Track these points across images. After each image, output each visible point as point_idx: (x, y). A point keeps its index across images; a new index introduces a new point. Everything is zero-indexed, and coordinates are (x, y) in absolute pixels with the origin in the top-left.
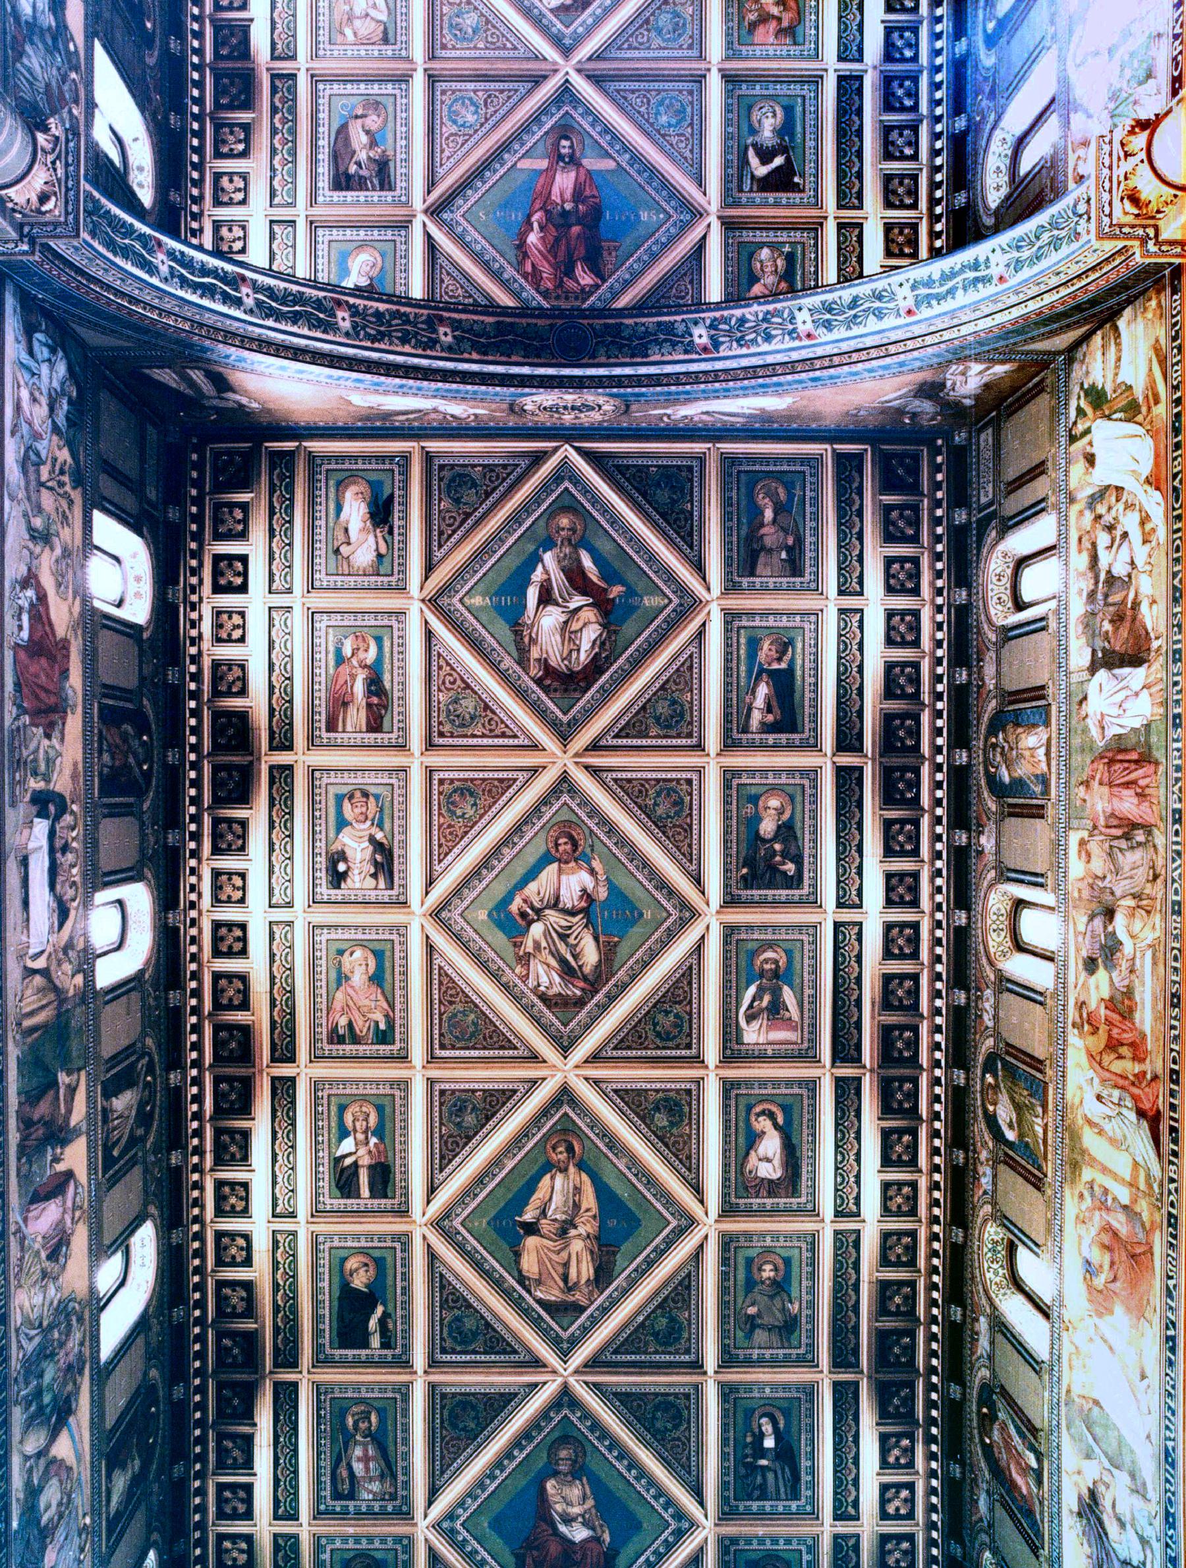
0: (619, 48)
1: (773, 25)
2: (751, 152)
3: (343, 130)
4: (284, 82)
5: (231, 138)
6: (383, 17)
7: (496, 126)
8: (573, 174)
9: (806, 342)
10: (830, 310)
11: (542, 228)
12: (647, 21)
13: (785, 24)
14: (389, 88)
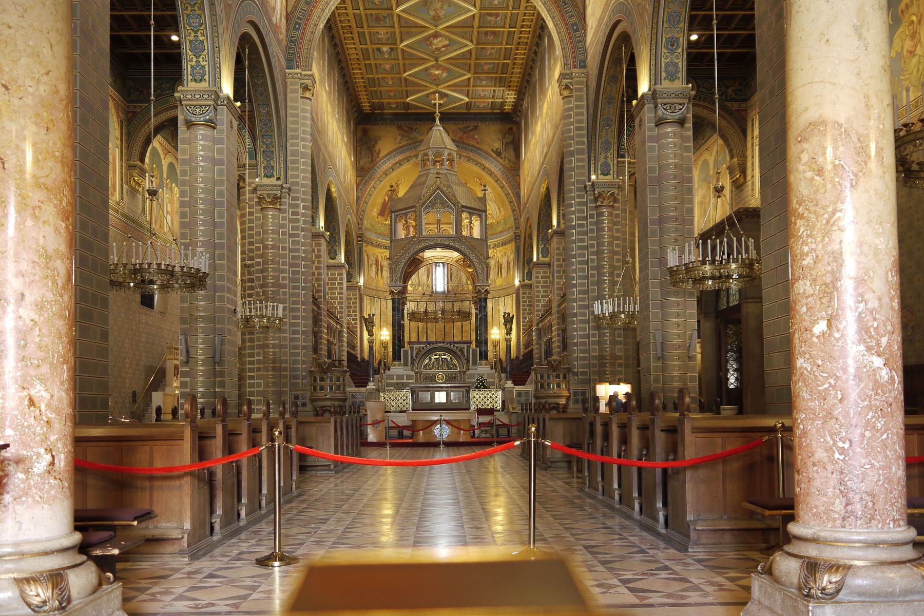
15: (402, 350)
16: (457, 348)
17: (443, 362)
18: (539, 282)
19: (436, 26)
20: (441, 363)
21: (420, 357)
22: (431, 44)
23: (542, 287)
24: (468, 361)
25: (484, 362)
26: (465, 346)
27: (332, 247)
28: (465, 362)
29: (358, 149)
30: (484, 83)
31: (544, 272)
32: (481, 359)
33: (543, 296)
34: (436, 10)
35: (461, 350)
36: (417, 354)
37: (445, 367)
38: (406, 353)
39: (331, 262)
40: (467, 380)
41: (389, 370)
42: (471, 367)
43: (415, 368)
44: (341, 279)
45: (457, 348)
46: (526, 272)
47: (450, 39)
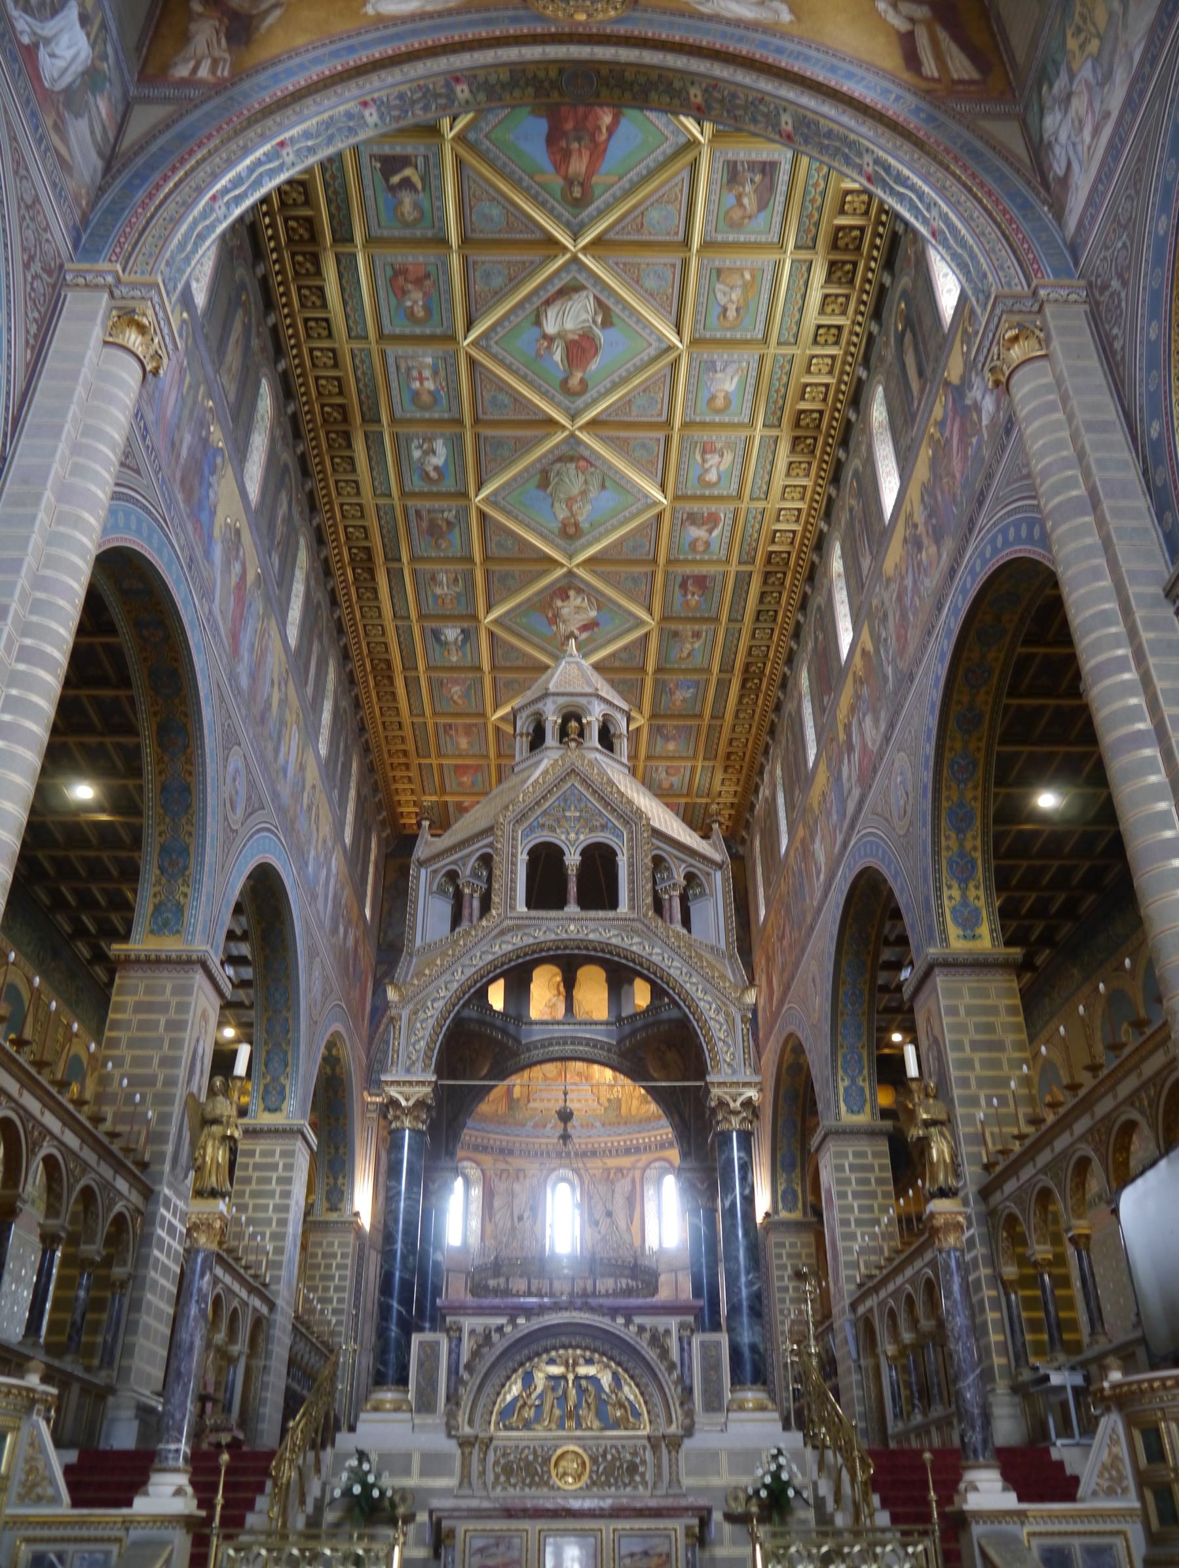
0: (532, 263)
1: (411, 277)
2: (419, 186)
3: (763, 205)
4: (807, 244)
5: (856, 205)
6: (719, 286)
7: (635, 207)
8: (571, 170)
9: (368, 98)
10: (350, 129)
11: (599, 128)
12: (510, 280)
13: (401, 279)
14: (720, 238)
15: (416, 1338)
16: (642, 1329)
17: (581, 1391)
18: (847, 1181)
19: (570, 557)
20: (572, 1393)
21: (482, 1367)
22: (555, 619)
23: (856, 1195)
24: (689, 1391)
25: (752, 1395)
26: (673, 1323)
27: (275, 1079)
28: (674, 1393)
29: (386, 906)
30: (671, 746)
31: (857, 1155)
32: (737, 1380)
33: (859, 1223)
34: (570, 501)
35: (657, 1340)
36: (476, 1354)
37: (591, 1419)
38: (431, 1351)
39: (266, 1119)
40: (687, 1481)
41: (352, 1429)
42: (700, 1417)
43: (462, 1417)
44: (289, 1167)
45: (642, 1329)
46: (780, 1189)
47: (601, 602)
